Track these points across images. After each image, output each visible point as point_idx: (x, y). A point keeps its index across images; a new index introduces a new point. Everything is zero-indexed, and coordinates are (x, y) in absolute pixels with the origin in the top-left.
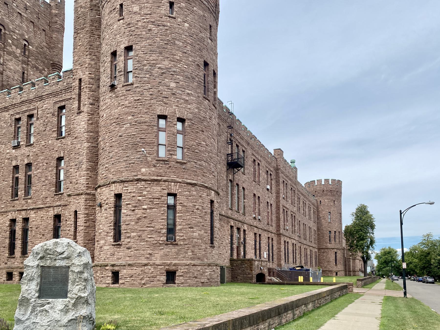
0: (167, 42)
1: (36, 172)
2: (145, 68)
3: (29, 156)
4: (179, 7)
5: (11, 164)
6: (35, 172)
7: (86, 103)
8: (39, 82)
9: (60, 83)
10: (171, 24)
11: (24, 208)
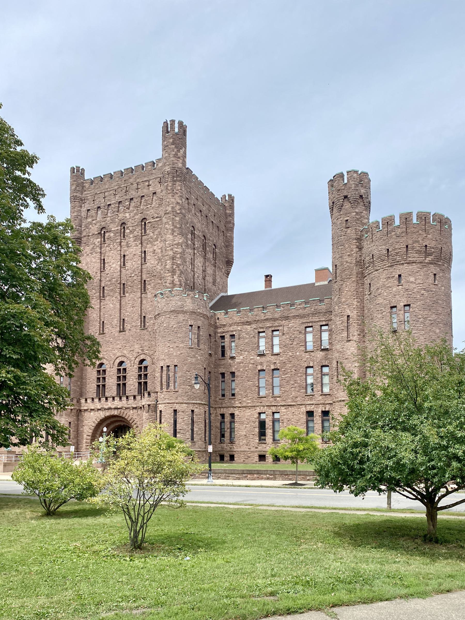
2: (420, 320)
5: (256, 368)
7: (355, 334)
9: (307, 308)
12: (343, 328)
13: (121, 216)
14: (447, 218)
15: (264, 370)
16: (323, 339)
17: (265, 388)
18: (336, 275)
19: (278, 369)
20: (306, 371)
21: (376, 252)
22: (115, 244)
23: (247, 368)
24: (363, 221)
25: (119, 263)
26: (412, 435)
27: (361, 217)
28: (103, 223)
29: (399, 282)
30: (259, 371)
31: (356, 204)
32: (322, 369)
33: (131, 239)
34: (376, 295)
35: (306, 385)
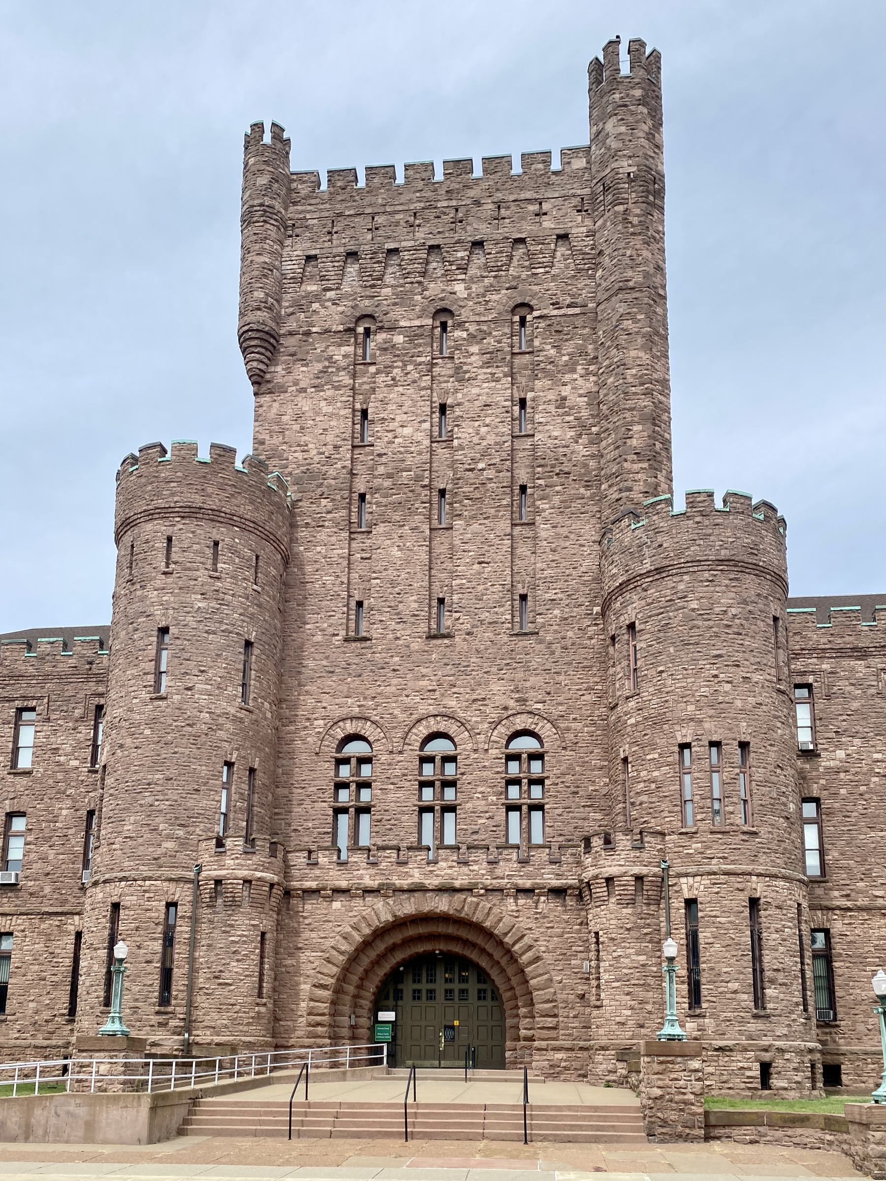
13: (434, 288)
22: (410, 368)
25: (427, 425)
28: (367, 302)
33: (473, 358)
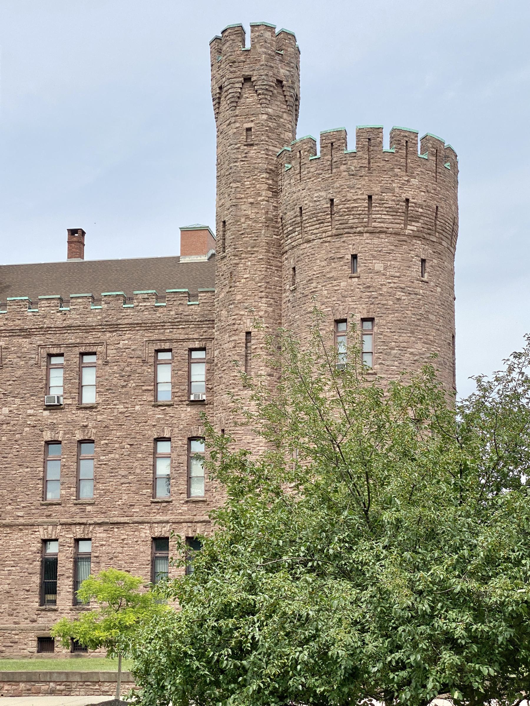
0: (420, 317)
1: (104, 457)
3: (86, 426)
4: (432, 266)
5: (40, 436)
6: (102, 458)
7: (263, 373)
8: (110, 299)
10: (424, 291)
11: (78, 520)
12: (236, 358)
14: (449, 148)
15: (59, 443)
16: (193, 379)
17: (58, 484)
18: (224, 243)
19: (92, 442)
20: (155, 448)
21: (306, 203)
23: (18, 436)
24: (282, 136)
26: (357, 585)
27: (279, 126)
29: (354, 270)
30: (48, 443)
31: (269, 98)
32: (189, 445)
34: (306, 293)
35: (155, 479)
